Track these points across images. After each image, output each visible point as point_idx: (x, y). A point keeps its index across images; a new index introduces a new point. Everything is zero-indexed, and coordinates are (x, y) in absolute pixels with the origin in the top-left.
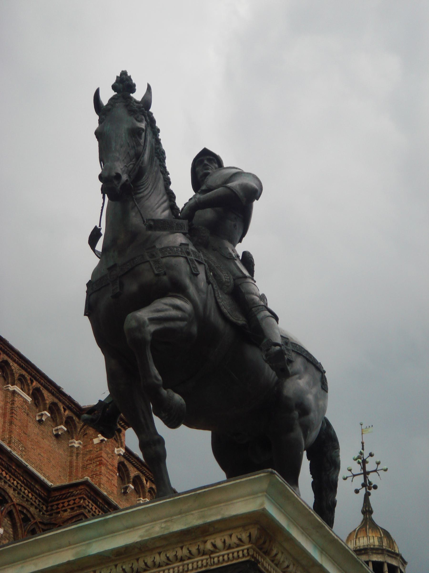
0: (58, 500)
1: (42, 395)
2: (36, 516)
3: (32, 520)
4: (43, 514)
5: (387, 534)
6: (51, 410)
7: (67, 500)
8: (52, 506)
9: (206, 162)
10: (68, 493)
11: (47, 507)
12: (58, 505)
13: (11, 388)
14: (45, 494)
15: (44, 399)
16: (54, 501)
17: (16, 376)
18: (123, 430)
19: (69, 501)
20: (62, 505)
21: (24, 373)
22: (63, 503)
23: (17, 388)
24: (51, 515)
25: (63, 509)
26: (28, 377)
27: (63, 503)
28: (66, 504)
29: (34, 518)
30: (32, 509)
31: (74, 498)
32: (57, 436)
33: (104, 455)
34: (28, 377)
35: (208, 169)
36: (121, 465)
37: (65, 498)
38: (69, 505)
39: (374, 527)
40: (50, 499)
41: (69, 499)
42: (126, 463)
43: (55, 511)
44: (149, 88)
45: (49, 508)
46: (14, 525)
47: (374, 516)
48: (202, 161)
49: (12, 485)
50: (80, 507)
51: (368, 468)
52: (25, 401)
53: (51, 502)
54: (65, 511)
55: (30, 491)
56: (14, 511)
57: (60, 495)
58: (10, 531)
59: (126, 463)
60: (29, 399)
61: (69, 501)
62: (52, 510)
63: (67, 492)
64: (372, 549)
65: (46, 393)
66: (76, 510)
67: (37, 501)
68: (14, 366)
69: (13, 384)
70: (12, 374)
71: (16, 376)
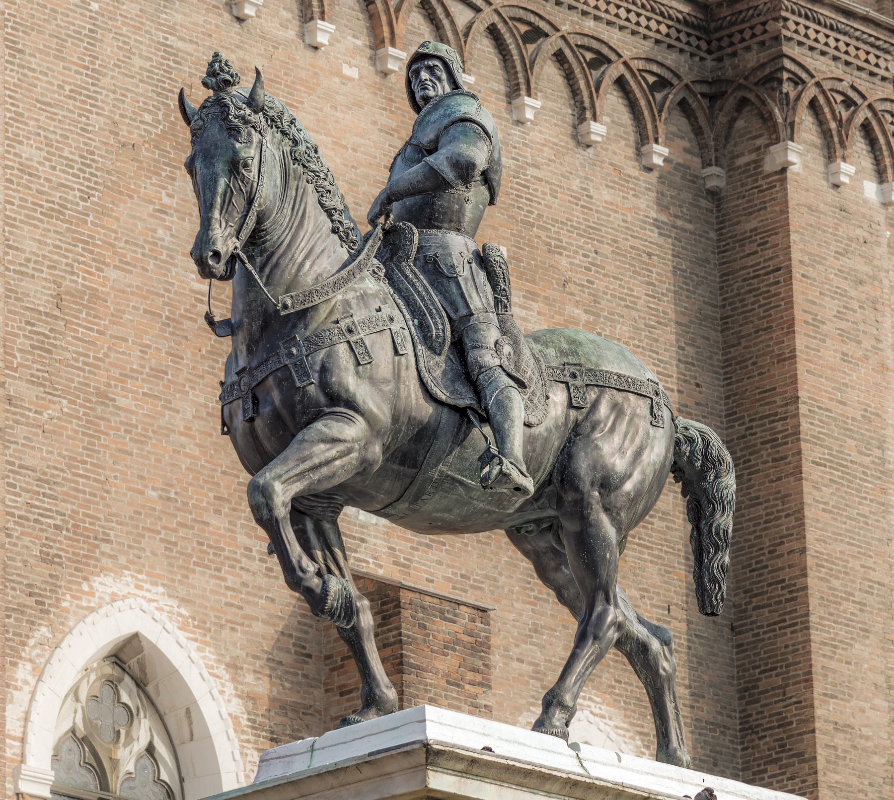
0: (732, 24)
2: (682, 71)
3: (675, 81)
4: (702, 59)
7: (748, 25)
8: (719, 40)
9: (424, 75)
10: (748, 9)
11: (709, 43)
12: (730, 36)
14: (699, 15)
16: (721, 28)
19: (752, 28)
20: (739, 36)
22: (741, 32)
24: (720, 60)
25: (745, 44)
27: (741, 32)
28: (747, 34)
29: (678, 77)
31: (762, 19)
35: (426, 89)
37: (743, 21)
38: (754, 35)
40: (713, 25)
41: (755, 21)
43: (729, 50)
44: (258, 72)
45: (714, 44)
48: (417, 73)
49: (614, 19)
53: (717, 30)
54: (748, 49)
55: (660, 19)
56: (628, 76)
57: (733, 14)
61: (752, 28)
62: (721, 48)
63: (746, 7)
66: (771, 47)
67: (683, 36)
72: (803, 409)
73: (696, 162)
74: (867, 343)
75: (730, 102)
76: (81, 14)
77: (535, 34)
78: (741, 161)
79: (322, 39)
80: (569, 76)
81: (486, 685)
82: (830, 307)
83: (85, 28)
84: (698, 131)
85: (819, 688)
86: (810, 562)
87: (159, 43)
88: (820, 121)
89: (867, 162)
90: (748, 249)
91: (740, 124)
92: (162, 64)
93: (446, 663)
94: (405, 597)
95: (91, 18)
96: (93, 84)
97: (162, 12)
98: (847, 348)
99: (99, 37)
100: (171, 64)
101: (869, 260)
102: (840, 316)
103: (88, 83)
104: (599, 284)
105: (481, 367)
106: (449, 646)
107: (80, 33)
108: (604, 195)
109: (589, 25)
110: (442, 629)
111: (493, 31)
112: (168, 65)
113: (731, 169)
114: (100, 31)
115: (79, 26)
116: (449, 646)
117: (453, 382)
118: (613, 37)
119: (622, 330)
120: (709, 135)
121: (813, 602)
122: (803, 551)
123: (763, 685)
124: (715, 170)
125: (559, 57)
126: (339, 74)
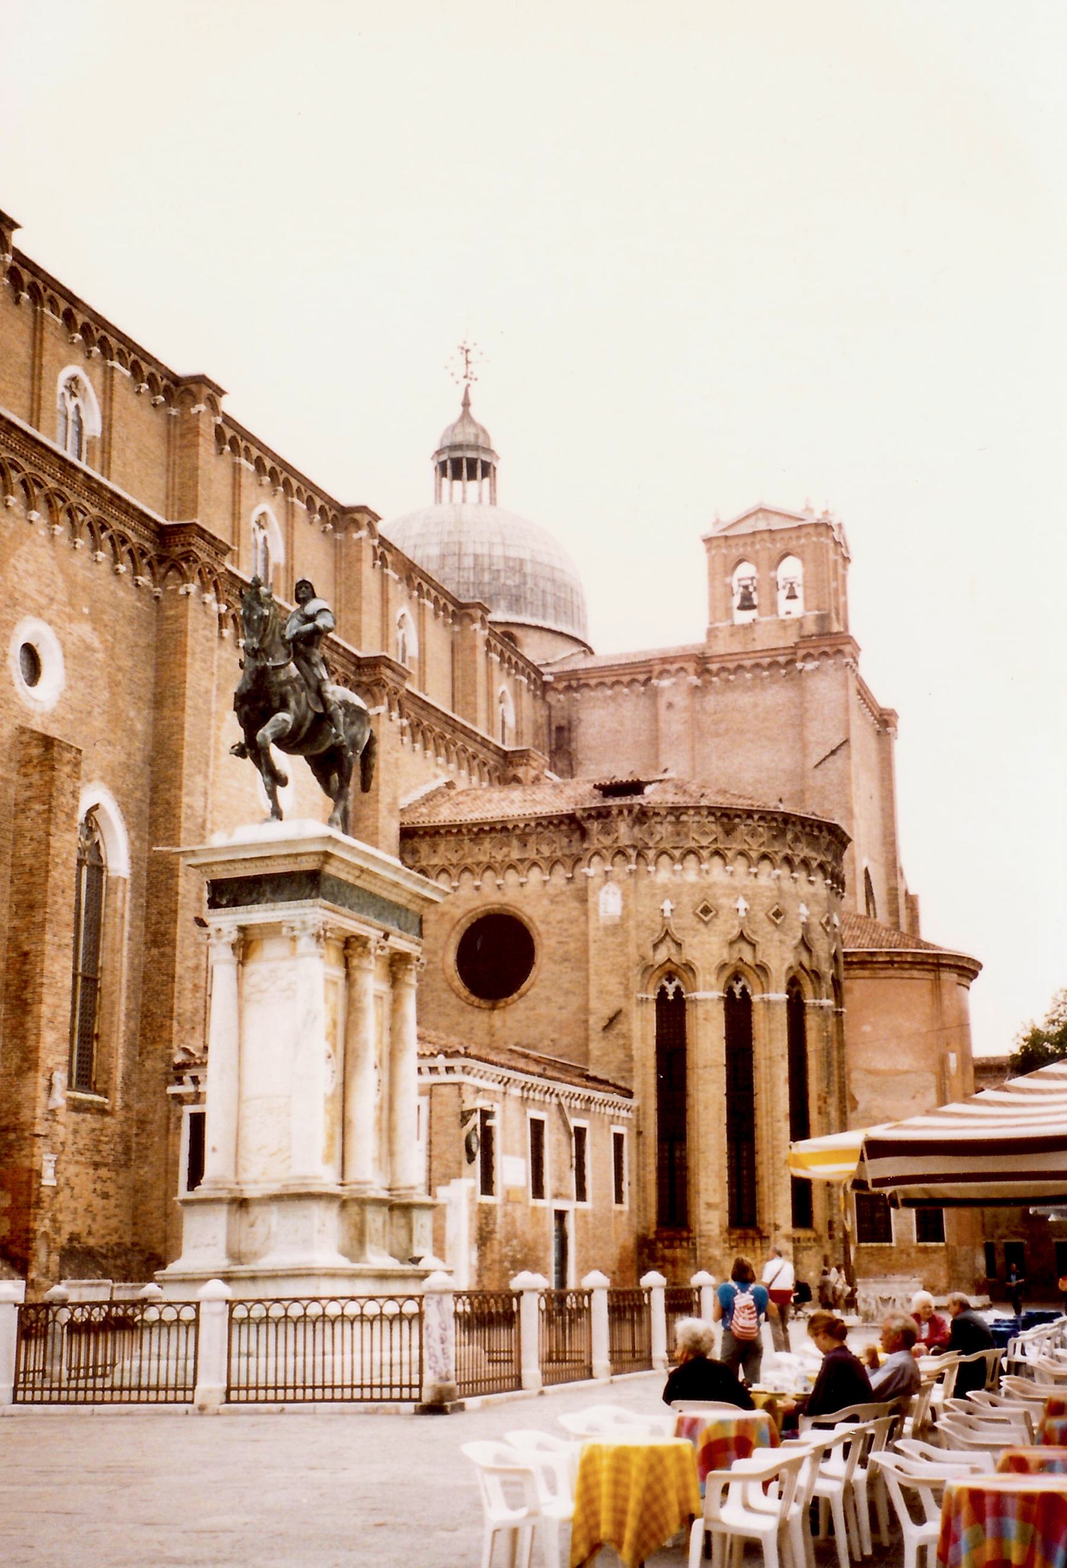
1: (140, 367)
5: (484, 431)
6: (150, 383)
13: (110, 363)
15: (141, 371)
17: (115, 351)
18: (217, 397)
21: (122, 346)
23: (116, 364)
26: (126, 350)
30: (147, 545)
32: (155, 405)
33: (201, 425)
34: (126, 350)
36: (218, 428)
39: (472, 422)
42: (223, 425)
46: (133, 561)
47: (473, 410)
50: (190, 544)
51: (471, 356)
52: (124, 376)
58: (131, 565)
59: (223, 425)
60: (128, 373)
64: (467, 446)
65: (143, 365)
68: (113, 341)
69: (112, 360)
70: (111, 350)
71: (115, 351)
72: (187, 685)
73: (151, 585)
74: (209, 664)
75: (168, 564)
77: (103, 528)
78: (170, 588)
79: (33, 518)
80: (113, 545)
81: (78, 779)
82: (198, 649)
84: (153, 574)
85: (184, 791)
86: (185, 744)
88: (201, 578)
89: (214, 595)
90: (169, 622)
91: (170, 573)
93: (67, 769)
94: (56, 743)
98: (203, 665)
101: (211, 632)
102: (201, 653)
104: (117, 628)
106: (69, 762)
108: (121, 594)
109: (121, 528)
110: (68, 756)
111: (90, 525)
113: (165, 591)
116: (69, 762)
118: (129, 533)
119: (123, 646)
120: (158, 577)
121: (185, 759)
122: (183, 739)
123: (161, 786)
124: (158, 589)
125: (111, 538)
126: (37, 533)
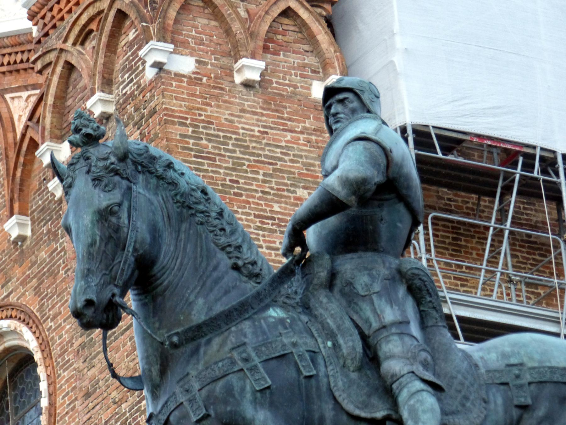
76: (444, 226)
83: (448, 237)
87: (522, 241)
92: (528, 259)
95: (453, 228)
96: (462, 285)
97: (522, 214)
99: (463, 243)
100: (537, 257)
103: (457, 285)
105: (392, 376)
107: (444, 242)
112: (534, 259)
114: (463, 238)
115: (443, 236)
117: (369, 396)
